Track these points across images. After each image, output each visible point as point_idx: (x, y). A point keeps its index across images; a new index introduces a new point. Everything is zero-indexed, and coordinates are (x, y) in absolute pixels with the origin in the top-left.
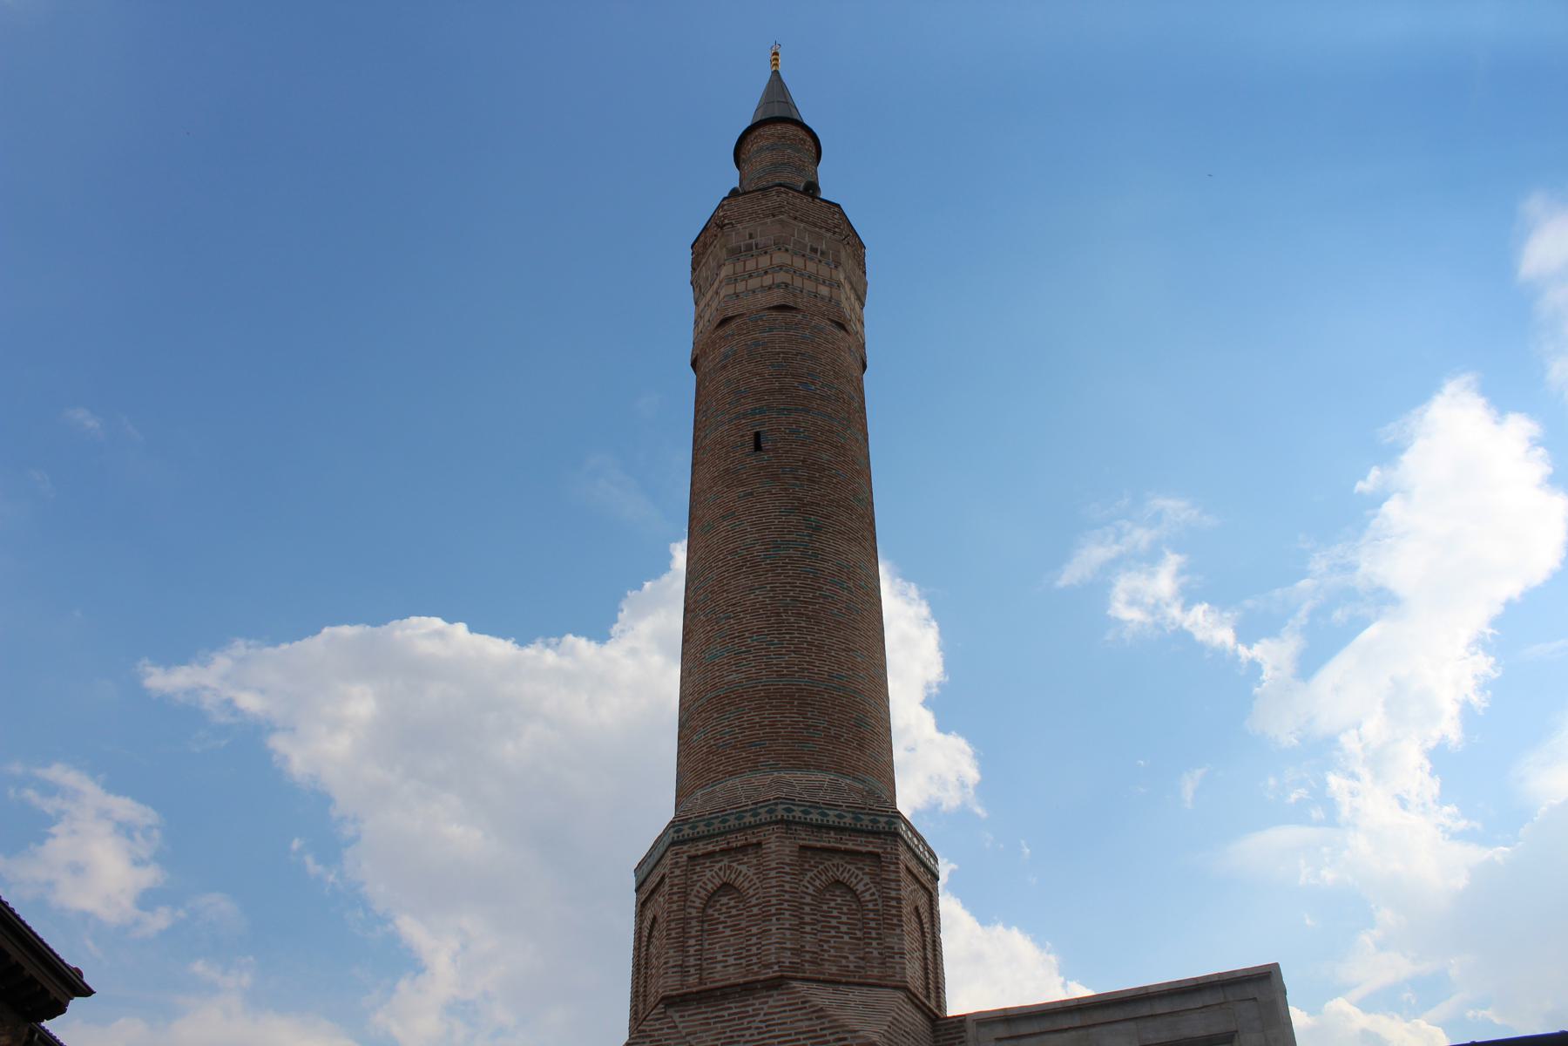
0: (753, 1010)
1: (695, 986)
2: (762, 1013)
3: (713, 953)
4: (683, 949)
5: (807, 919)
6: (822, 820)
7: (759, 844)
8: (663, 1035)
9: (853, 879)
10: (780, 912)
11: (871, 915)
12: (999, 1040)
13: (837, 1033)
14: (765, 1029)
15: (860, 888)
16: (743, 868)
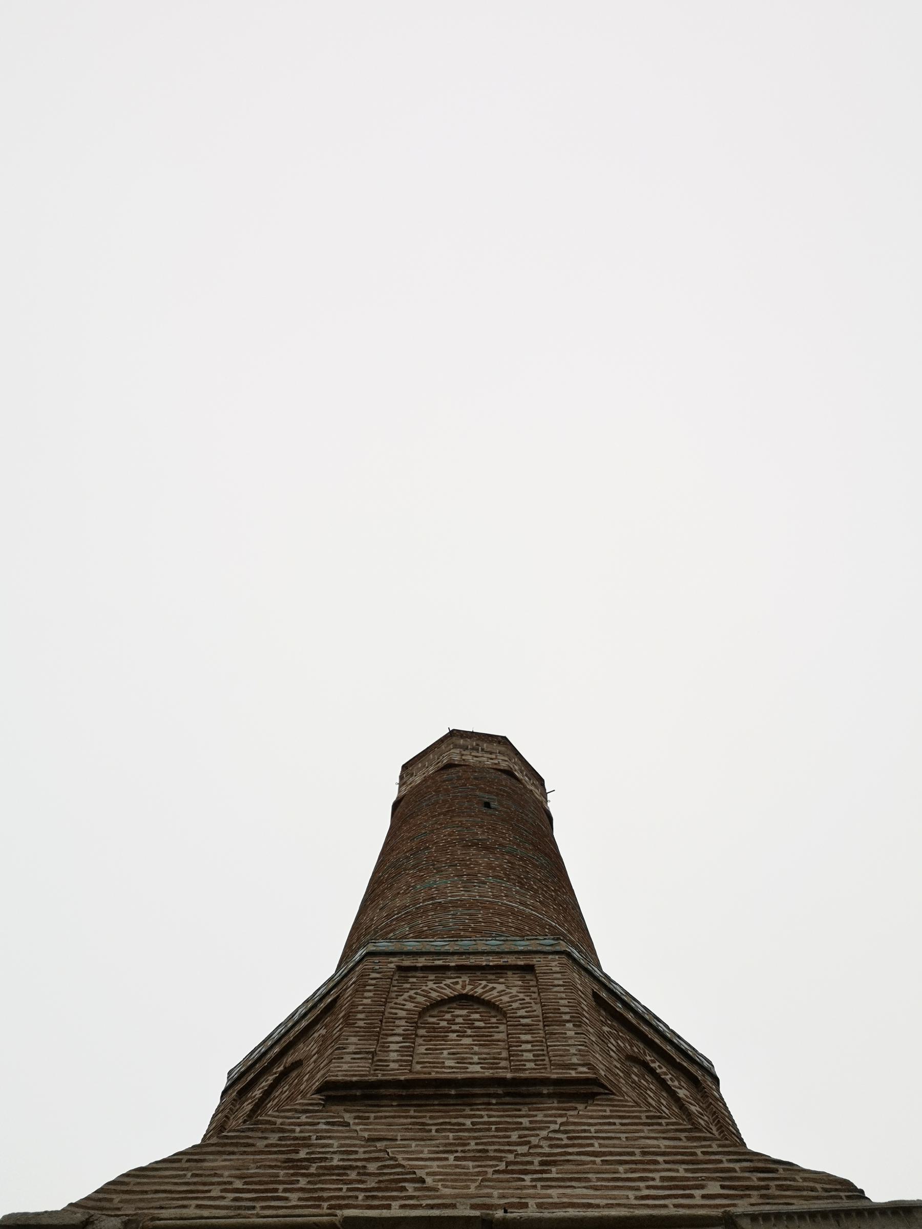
8: (316, 1131)
14: (566, 1142)
16: (500, 987)
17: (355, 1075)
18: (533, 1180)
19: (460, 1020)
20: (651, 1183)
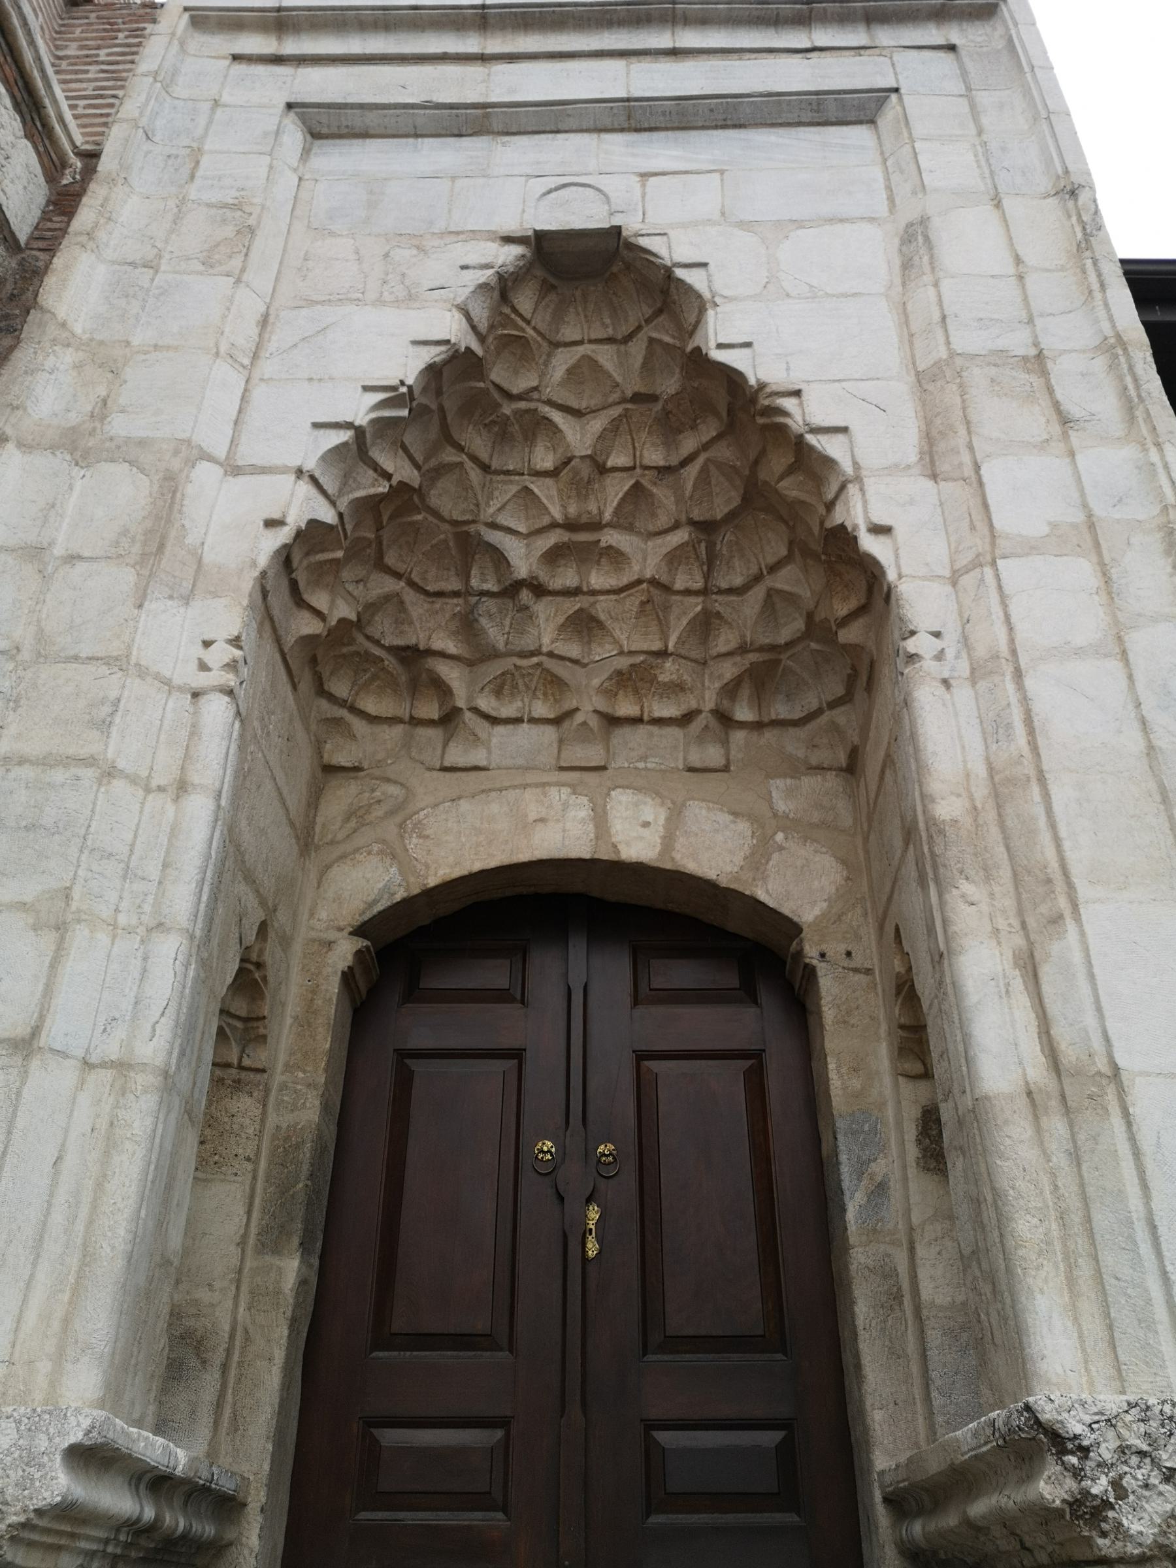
12: (236, 58)
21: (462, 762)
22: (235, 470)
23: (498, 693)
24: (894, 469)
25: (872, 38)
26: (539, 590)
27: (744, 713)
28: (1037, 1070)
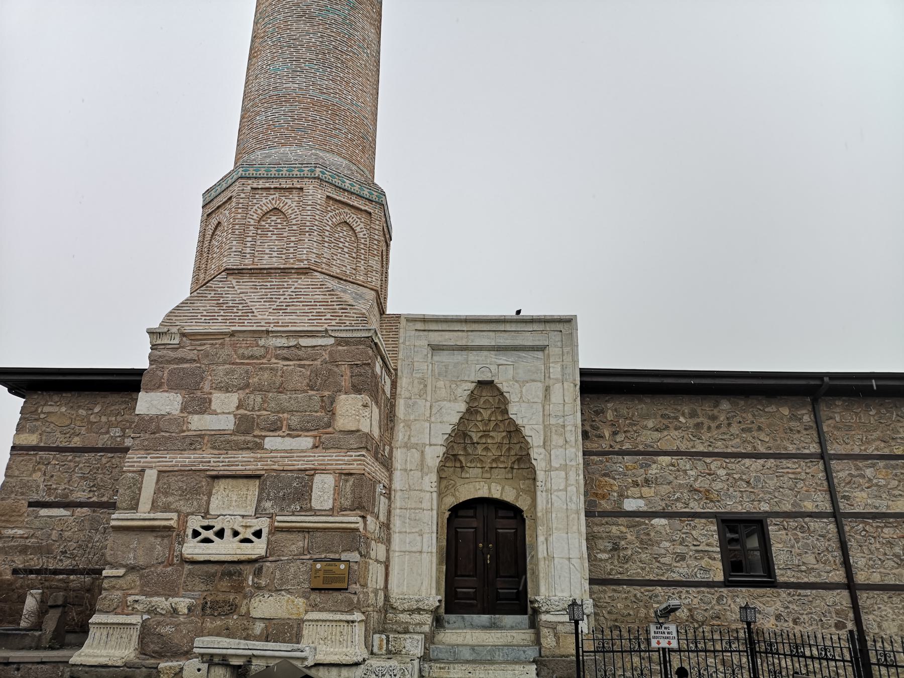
0: (287, 285)
1: (249, 265)
2: (293, 287)
3: (263, 248)
4: (242, 239)
5: (326, 239)
6: (341, 184)
7: (301, 189)
8: (224, 291)
9: (354, 223)
10: (311, 232)
11: (362, 246)
13: (342, 305)
14: (294, 297)
15: (358, 229)
16: (289, 201)
17: (235, 265)
18: (283, 313)
19: (273, 224)
20: (313, 314)
21: (464, 477)
22: (431, 445)
23: (471, 462)
24: (538, 446)
25: (545, 327)
26: (478, 443)
27: (516, 467)
28: (545, 555)
